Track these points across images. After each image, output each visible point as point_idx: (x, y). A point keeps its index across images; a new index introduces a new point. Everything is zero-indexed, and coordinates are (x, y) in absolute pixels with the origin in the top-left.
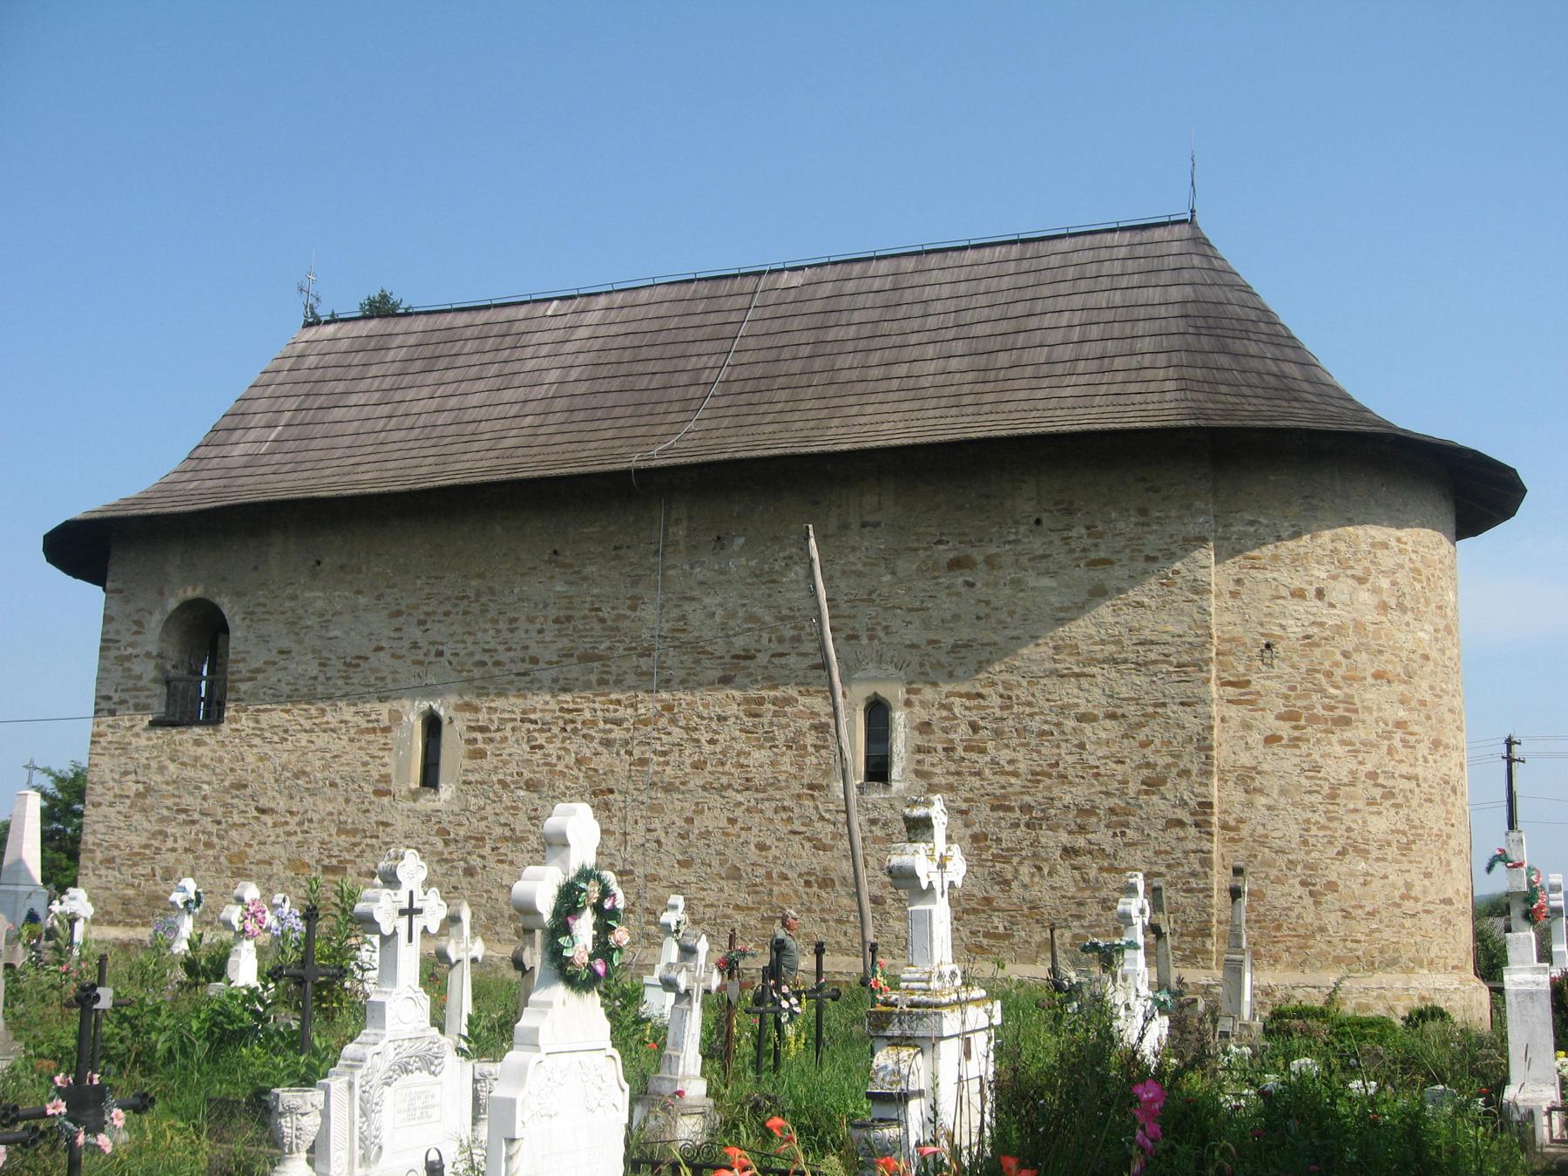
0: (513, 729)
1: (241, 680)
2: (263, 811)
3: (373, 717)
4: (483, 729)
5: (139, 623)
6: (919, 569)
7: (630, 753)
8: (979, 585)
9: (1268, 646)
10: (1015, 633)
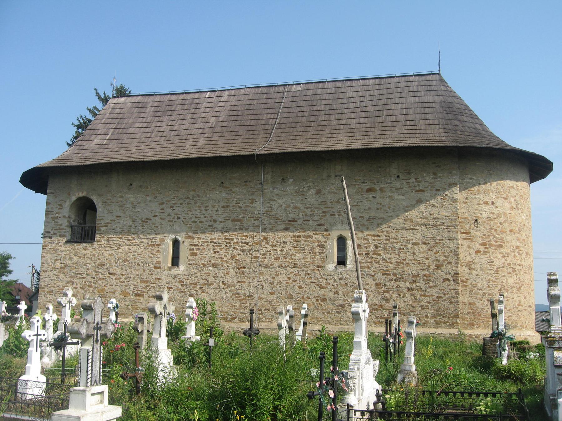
0: (207, 245)
1: (102, 227)
2: (111, 274)
3: (153, 240)
4: (195, 245)
5: (60, 205)
6: (356, 192)
7: (251, 254)
8: (377, 197)
9: (476, 220)
10: (390, 215)
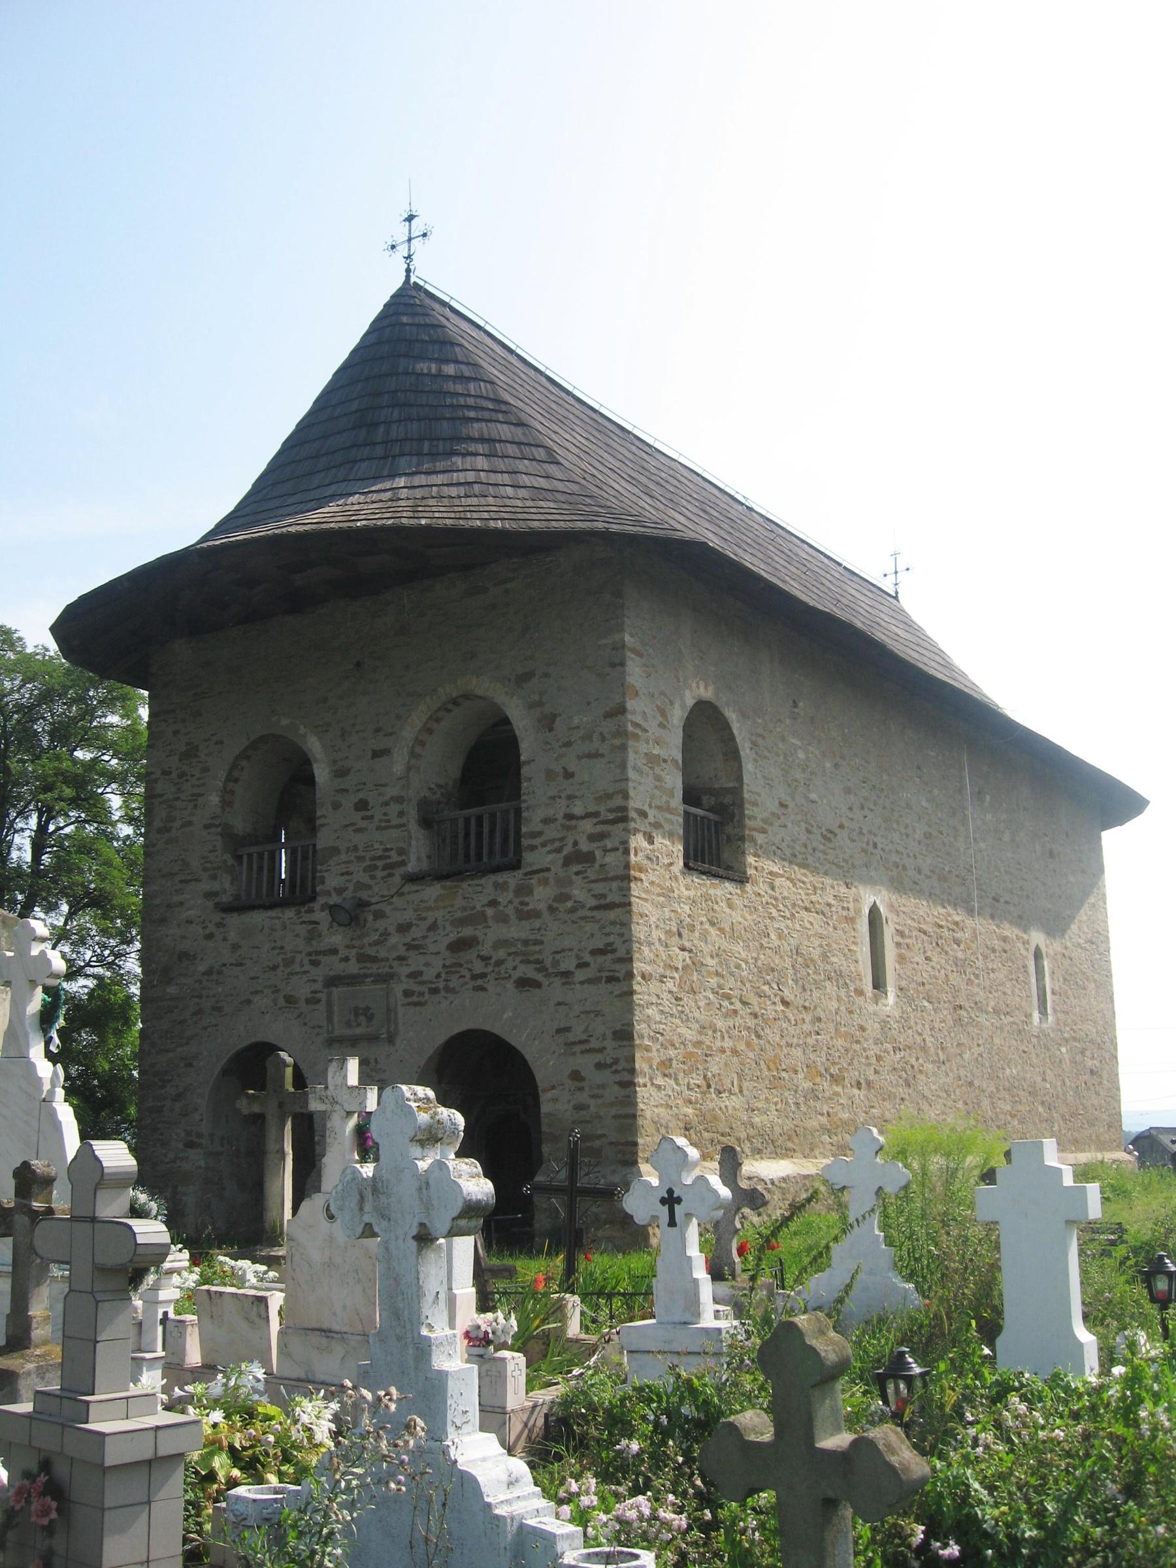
1: (755, 829)
5: (663, 713)
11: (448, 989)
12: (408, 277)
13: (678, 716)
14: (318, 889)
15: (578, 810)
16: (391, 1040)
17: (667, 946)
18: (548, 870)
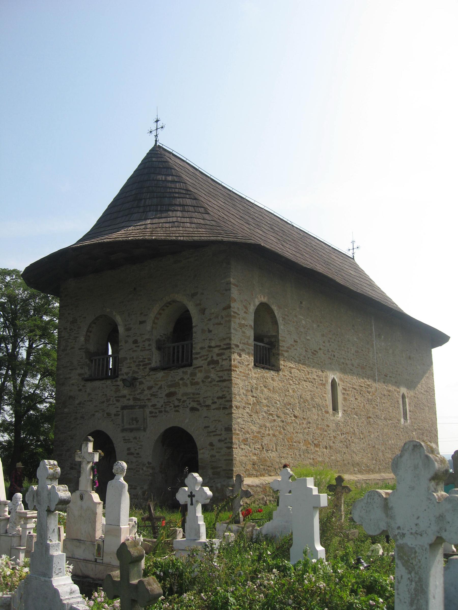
5: (246, 308)
11: (166, 411)
12: (156, 143)
13: (252, 309)
14: (119, 373)
15: (213, 344)
16: (145, 430)
17: (246, 395)
18: (202, 367)
